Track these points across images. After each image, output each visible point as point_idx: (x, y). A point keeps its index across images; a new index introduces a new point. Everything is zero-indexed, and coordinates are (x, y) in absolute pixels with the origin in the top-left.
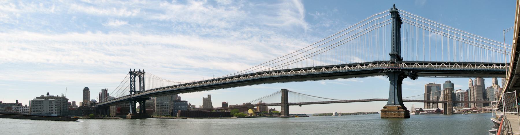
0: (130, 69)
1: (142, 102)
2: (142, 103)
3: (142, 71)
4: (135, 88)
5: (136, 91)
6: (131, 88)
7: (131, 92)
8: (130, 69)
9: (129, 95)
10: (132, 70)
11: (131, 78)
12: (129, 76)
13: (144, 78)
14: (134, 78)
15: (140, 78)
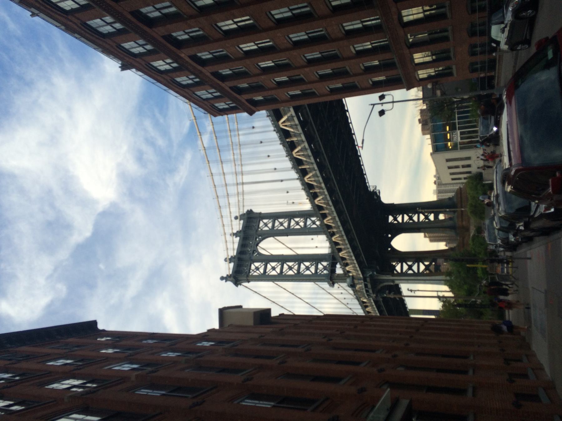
0: (222, 278)
1: (391, 218)
2: (395, 219)
3: (238, 226)
4: (316, 259)
5: (333, 252)
6: (315, 278)
7: (332, 279)
8: (222, 278)
9: (352, 286)
10: (228, 269)
11: (264, 277)
12: (252, 284)
13: (274, 216)
14: (267, 259)
15: (273, 233)
